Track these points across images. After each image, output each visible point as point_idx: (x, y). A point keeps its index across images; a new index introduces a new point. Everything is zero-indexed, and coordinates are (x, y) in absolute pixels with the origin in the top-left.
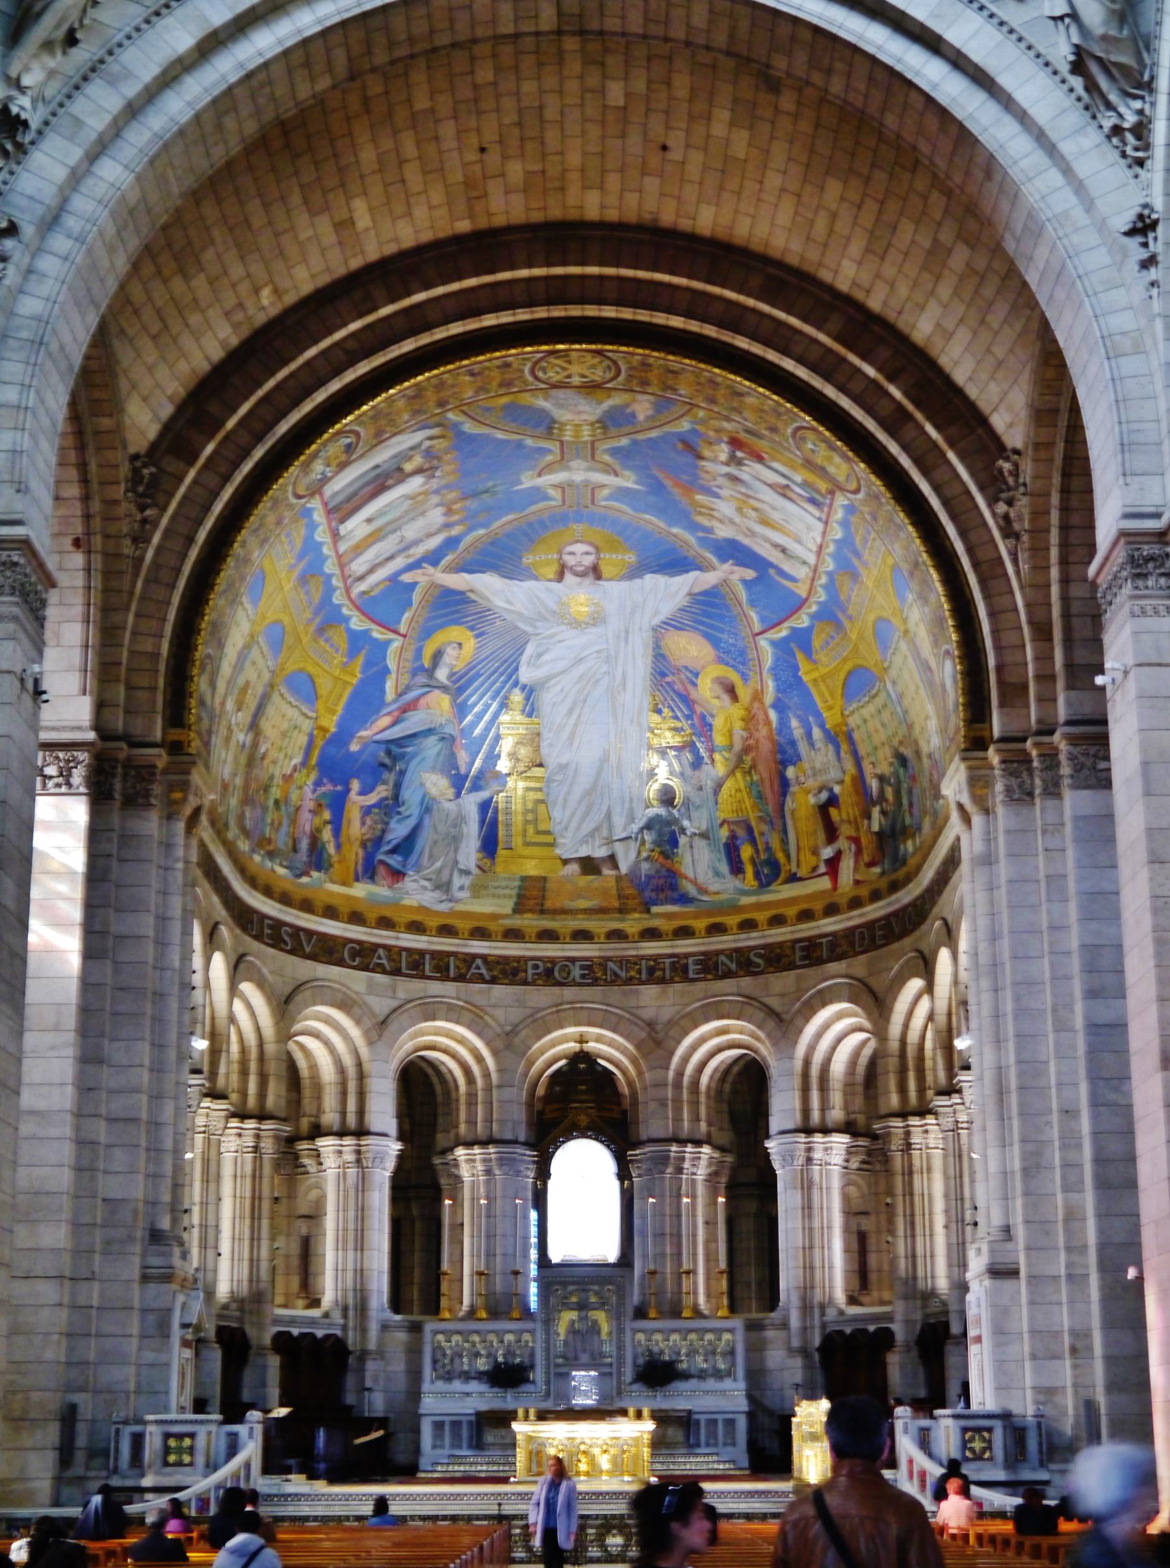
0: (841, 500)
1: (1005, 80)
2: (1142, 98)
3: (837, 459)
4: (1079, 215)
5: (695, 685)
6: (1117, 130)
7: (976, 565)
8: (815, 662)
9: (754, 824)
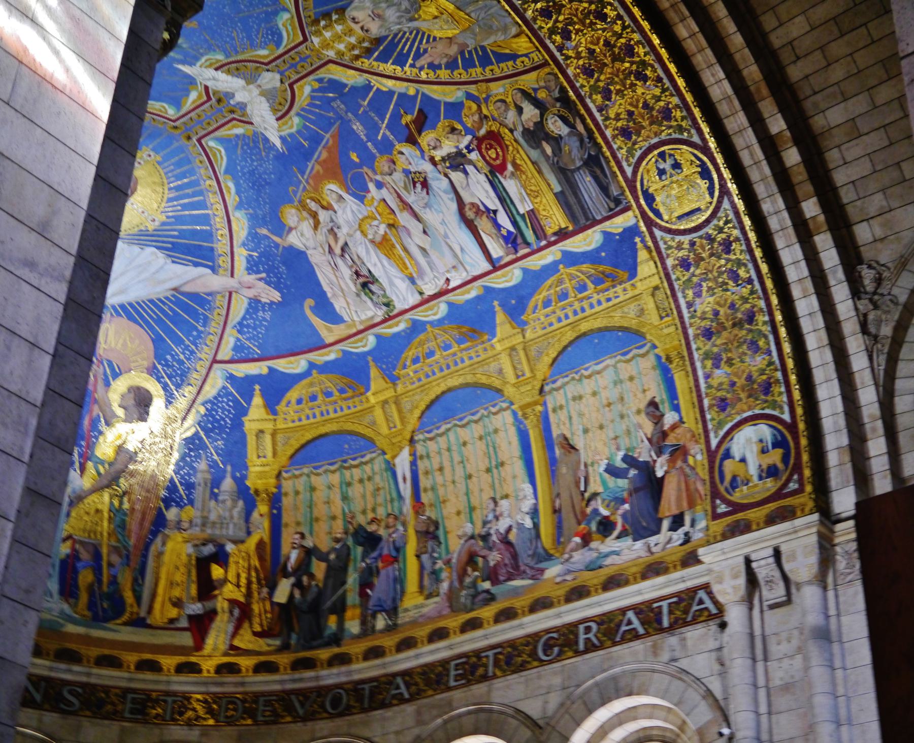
5: (108, 385)
8: (275, 413)
9: (104, 551)
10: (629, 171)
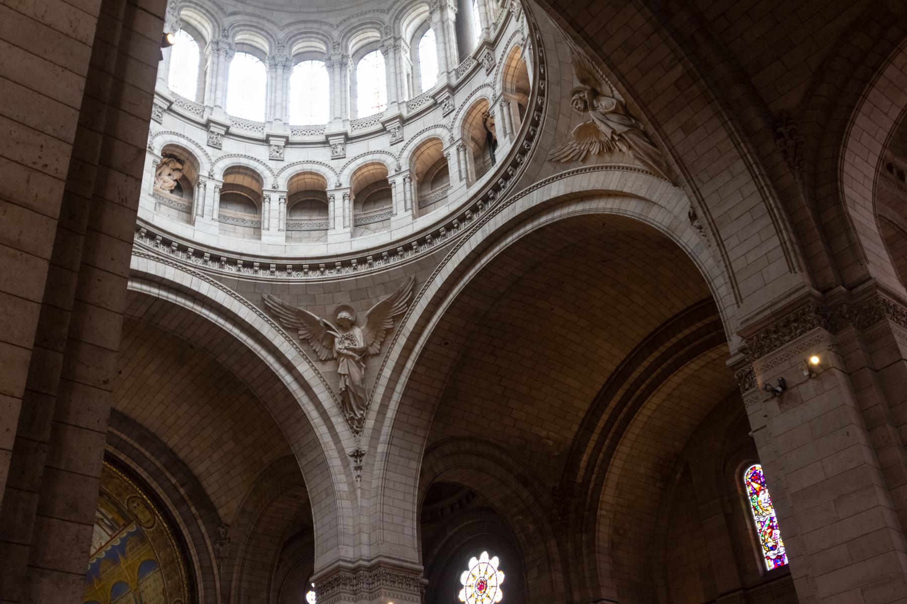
0: (133, 528)
1: (315, 390)
2: (364, 410)
3: (147, 512)
4: (332, 444)
6: (352, 419)
7: (201, 567)
10: (126, 507)
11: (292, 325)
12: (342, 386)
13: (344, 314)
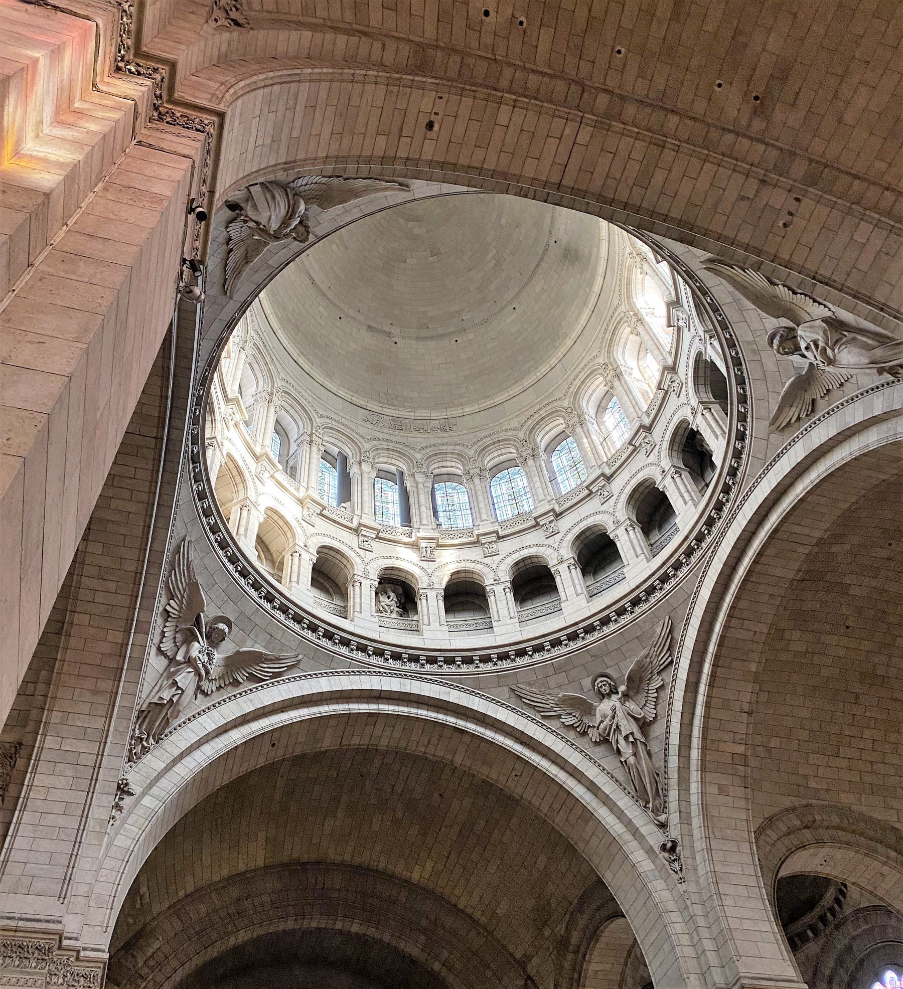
11: (174, 589)
12: (166, 695)
13: (227, 630)
